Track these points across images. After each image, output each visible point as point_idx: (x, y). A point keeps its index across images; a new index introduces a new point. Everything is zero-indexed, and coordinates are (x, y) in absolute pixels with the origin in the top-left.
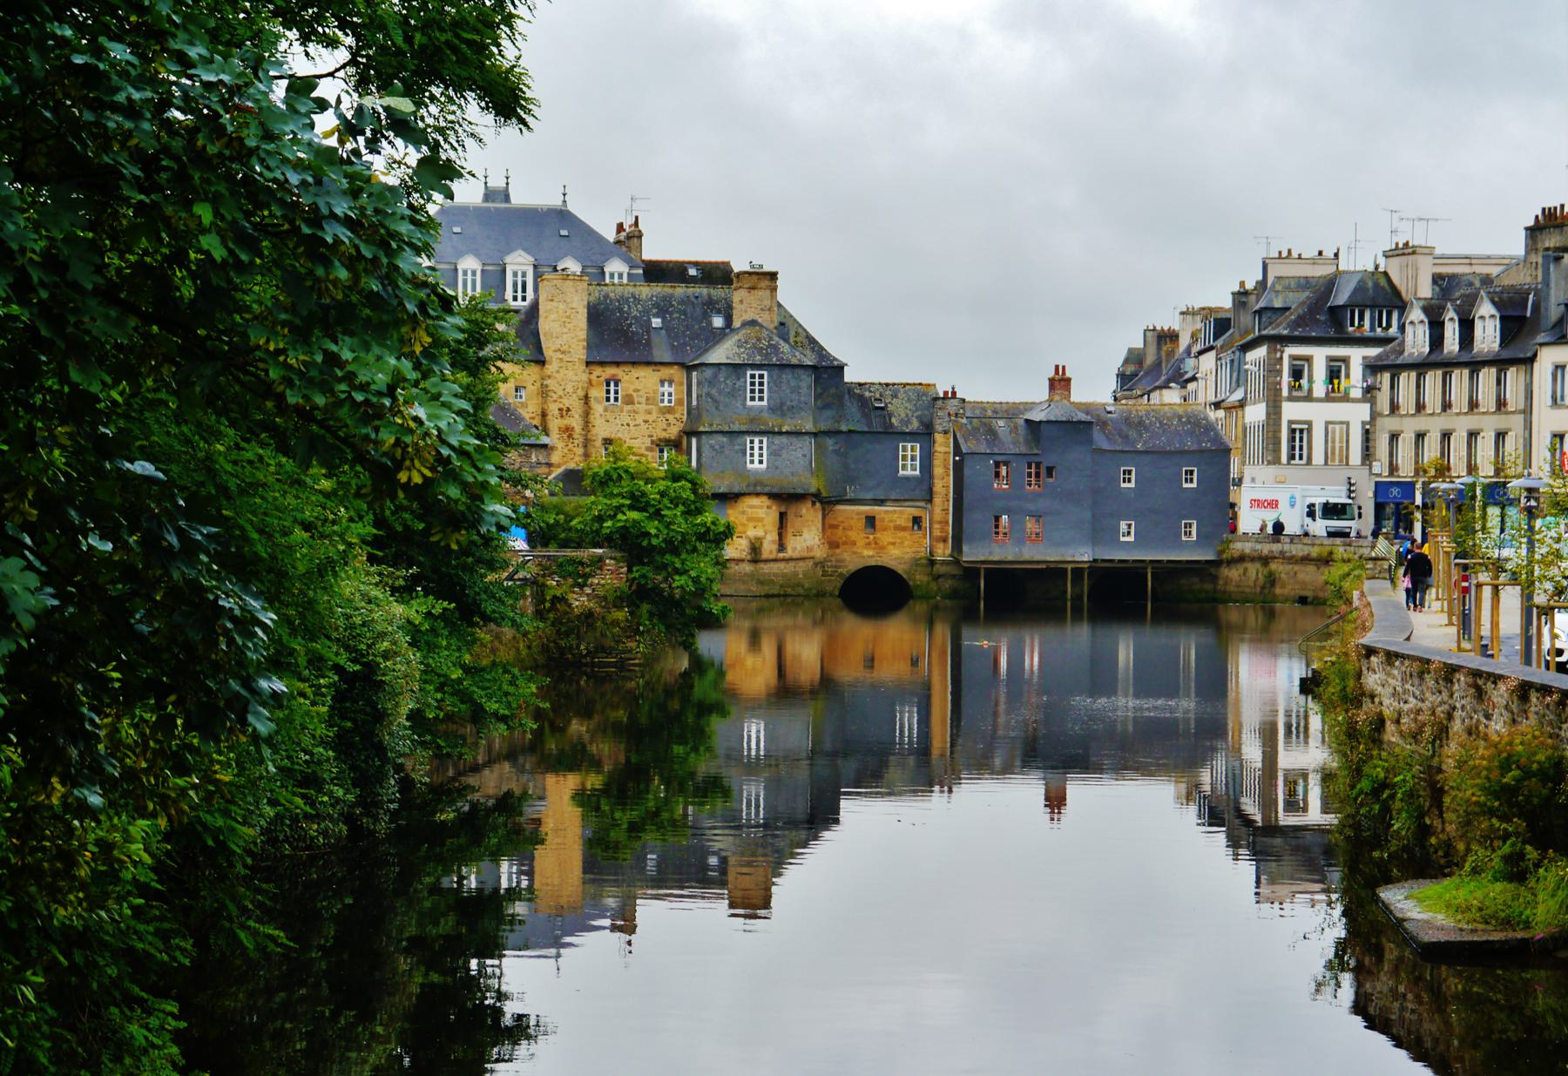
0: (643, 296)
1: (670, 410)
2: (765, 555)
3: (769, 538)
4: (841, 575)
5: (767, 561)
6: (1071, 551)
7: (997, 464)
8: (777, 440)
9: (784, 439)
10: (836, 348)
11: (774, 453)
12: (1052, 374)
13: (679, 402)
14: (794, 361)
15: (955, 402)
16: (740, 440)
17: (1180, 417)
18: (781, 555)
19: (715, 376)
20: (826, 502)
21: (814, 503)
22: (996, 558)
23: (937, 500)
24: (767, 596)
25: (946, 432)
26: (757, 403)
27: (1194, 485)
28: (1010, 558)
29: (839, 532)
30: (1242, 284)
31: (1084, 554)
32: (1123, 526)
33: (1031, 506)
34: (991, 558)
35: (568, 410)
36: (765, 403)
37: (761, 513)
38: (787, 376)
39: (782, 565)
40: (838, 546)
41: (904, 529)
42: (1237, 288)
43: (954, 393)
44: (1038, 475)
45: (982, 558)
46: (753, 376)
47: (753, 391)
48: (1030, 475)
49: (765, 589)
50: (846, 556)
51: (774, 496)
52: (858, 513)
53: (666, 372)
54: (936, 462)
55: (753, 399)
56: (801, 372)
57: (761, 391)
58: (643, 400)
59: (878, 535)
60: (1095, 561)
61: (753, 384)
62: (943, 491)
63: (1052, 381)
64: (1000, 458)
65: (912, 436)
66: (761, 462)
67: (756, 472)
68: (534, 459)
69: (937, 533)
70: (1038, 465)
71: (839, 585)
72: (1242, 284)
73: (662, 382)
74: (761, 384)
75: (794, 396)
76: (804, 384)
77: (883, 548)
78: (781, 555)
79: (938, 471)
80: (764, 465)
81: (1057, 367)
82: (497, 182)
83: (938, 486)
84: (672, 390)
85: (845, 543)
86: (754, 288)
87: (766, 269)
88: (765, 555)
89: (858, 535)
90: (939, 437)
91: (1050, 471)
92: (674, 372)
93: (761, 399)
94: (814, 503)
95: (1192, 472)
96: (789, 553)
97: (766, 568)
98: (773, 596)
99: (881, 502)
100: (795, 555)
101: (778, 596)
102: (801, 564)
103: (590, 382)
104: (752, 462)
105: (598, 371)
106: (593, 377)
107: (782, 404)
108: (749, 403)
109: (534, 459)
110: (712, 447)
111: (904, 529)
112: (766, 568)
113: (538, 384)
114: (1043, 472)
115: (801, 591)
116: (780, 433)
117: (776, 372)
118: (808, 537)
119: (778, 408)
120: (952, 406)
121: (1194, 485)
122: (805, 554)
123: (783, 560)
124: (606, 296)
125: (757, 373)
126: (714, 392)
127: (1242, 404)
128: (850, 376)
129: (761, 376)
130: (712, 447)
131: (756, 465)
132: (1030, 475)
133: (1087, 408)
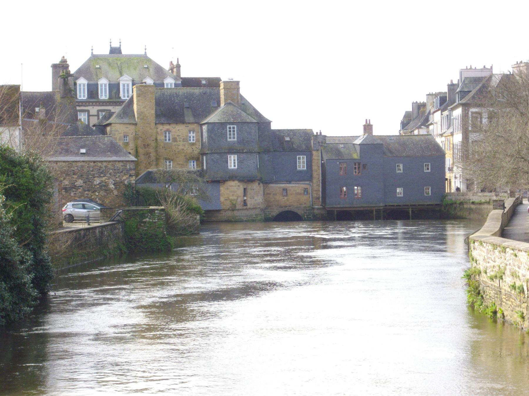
0: (181, 93)
1: (193, 144)
5: (238, 210)
8: (242, 156)
9: (244, 155)
10: (266, 114)
11: (240, 162)
12: (364, 123)
13: (197, 140)
14: (248, 121)
17: (423, 140)
20: (265, 182)
21: (259, 184)
23: (315, 181)
25: (317, 150)
26: (232, 140)
27: (429, 171)
29: (271, 196)
30: (452, 81)
32: (398, 190)
35: (148, 145)
36: (236, 139)
37: (235, 189)
42: (450, 83)
43: (321, 133)
46: (230, 128)
47: (230, 134)
48: (355, 168)
52: (279, 188)
53: (191, 127)
54: (313, 164)
55: (230, 138)
57: (234, 134)
58: (182, 140)
60: (386, 206)
61: (230, 131)
62: (317, 177)
63: (365, 126)
65: (302, 152)
66: (235, 166)
67: (233, 170)
68: (128, 167)
69: (315, 195)
70: (359, 164)
72: (452, 81)
73: (190, 132)
74: (234, 131)
78: (245, 207)
79: (315, 168)
80: (236, 167)
81: (366, 120)
82: (115, 45)
83: (315, 175)
84: (194, 135)
87: (235, 80)
88: (238, 207)
90: (314, 153)
91: (364, 166)
92: (195, 126)
93: (234, 138)
95: (428, 165)
96: (249, 206)
99: (289, 182)
100: (252, 207)
103: (157, 133)
106: (159, 130)
107: (243, 140)
108: (229, 140)
109: (128, 167)
111: (300, 194)
113: (134, 134)
114: (361, 166)
116: (243, 153)
119: (241, 141)
121: (429, 171)
123: (246, 209)
124: (164, 94)
125: (232, 126)
126: (213, 135)
127: (452, 134)
128: (274, 127)
129: (234, 128)
132: (355, 168)
133: (381, 138)
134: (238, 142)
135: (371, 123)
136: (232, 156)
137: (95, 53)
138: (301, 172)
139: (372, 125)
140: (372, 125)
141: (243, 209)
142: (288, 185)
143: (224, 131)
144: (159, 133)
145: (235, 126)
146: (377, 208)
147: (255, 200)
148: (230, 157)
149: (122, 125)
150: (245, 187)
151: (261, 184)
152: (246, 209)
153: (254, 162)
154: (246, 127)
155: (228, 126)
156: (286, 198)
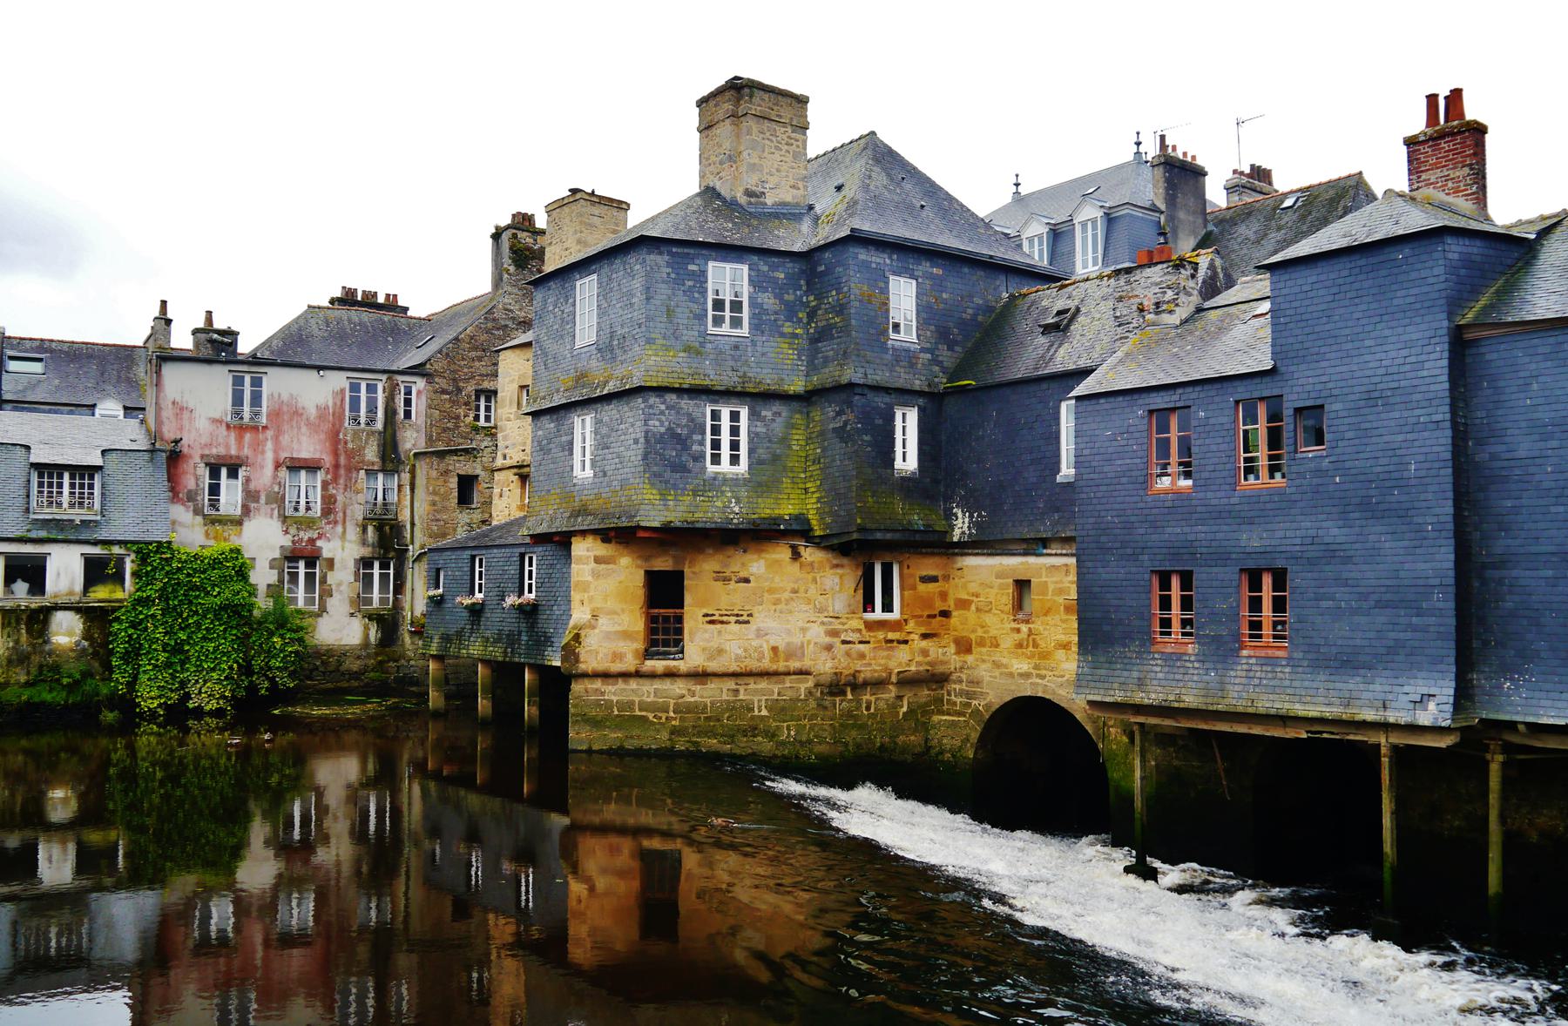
2: (588, 663)
3: (604, 623)
4: (976, 712)
5: (606, 676)
7: (1161, 416)
21: (796, 555)
22: (1152, 697)
24: (618, 753)
28: (1191, 700)
29: (971, 615)
31: (1422, 703)
33: (1253, 540)
34: (1140, 698)
39: (678, 687)
40: (969, 651)
45: (1118, 696)
49: (613, 737)
50: (984, 672)
51: (622, 535)
59: (1037, 625)
64: (1160, 401)
71: (975, 736)
76: (637, 284)
77: (1045, 656)
81: (1432, 99)
85: (981, 643)
86: (709, 127)
88: (588, 663)
89: (999, 624)
94: (796, 555)
97: (614, 692)
98: (640, 754)
100: (713, 666)
101: (666, 755)
102: (763, 684)
112: (614, 692)
115: (765, 746)
118: (781, 623)
122: (766, 664)
123: (671, 675)
135: (1471, 113)
136: (588, 419)
137: (1023, 190)
139: (1479, 130)
140: (1479, 130)
141: (638, 674)
142: (1031, 560)
147: (760, 634)
149: (518, 351)
150: (663, 564)
151: (810, 554)
152: (671, 675)
156: (1024, 628)
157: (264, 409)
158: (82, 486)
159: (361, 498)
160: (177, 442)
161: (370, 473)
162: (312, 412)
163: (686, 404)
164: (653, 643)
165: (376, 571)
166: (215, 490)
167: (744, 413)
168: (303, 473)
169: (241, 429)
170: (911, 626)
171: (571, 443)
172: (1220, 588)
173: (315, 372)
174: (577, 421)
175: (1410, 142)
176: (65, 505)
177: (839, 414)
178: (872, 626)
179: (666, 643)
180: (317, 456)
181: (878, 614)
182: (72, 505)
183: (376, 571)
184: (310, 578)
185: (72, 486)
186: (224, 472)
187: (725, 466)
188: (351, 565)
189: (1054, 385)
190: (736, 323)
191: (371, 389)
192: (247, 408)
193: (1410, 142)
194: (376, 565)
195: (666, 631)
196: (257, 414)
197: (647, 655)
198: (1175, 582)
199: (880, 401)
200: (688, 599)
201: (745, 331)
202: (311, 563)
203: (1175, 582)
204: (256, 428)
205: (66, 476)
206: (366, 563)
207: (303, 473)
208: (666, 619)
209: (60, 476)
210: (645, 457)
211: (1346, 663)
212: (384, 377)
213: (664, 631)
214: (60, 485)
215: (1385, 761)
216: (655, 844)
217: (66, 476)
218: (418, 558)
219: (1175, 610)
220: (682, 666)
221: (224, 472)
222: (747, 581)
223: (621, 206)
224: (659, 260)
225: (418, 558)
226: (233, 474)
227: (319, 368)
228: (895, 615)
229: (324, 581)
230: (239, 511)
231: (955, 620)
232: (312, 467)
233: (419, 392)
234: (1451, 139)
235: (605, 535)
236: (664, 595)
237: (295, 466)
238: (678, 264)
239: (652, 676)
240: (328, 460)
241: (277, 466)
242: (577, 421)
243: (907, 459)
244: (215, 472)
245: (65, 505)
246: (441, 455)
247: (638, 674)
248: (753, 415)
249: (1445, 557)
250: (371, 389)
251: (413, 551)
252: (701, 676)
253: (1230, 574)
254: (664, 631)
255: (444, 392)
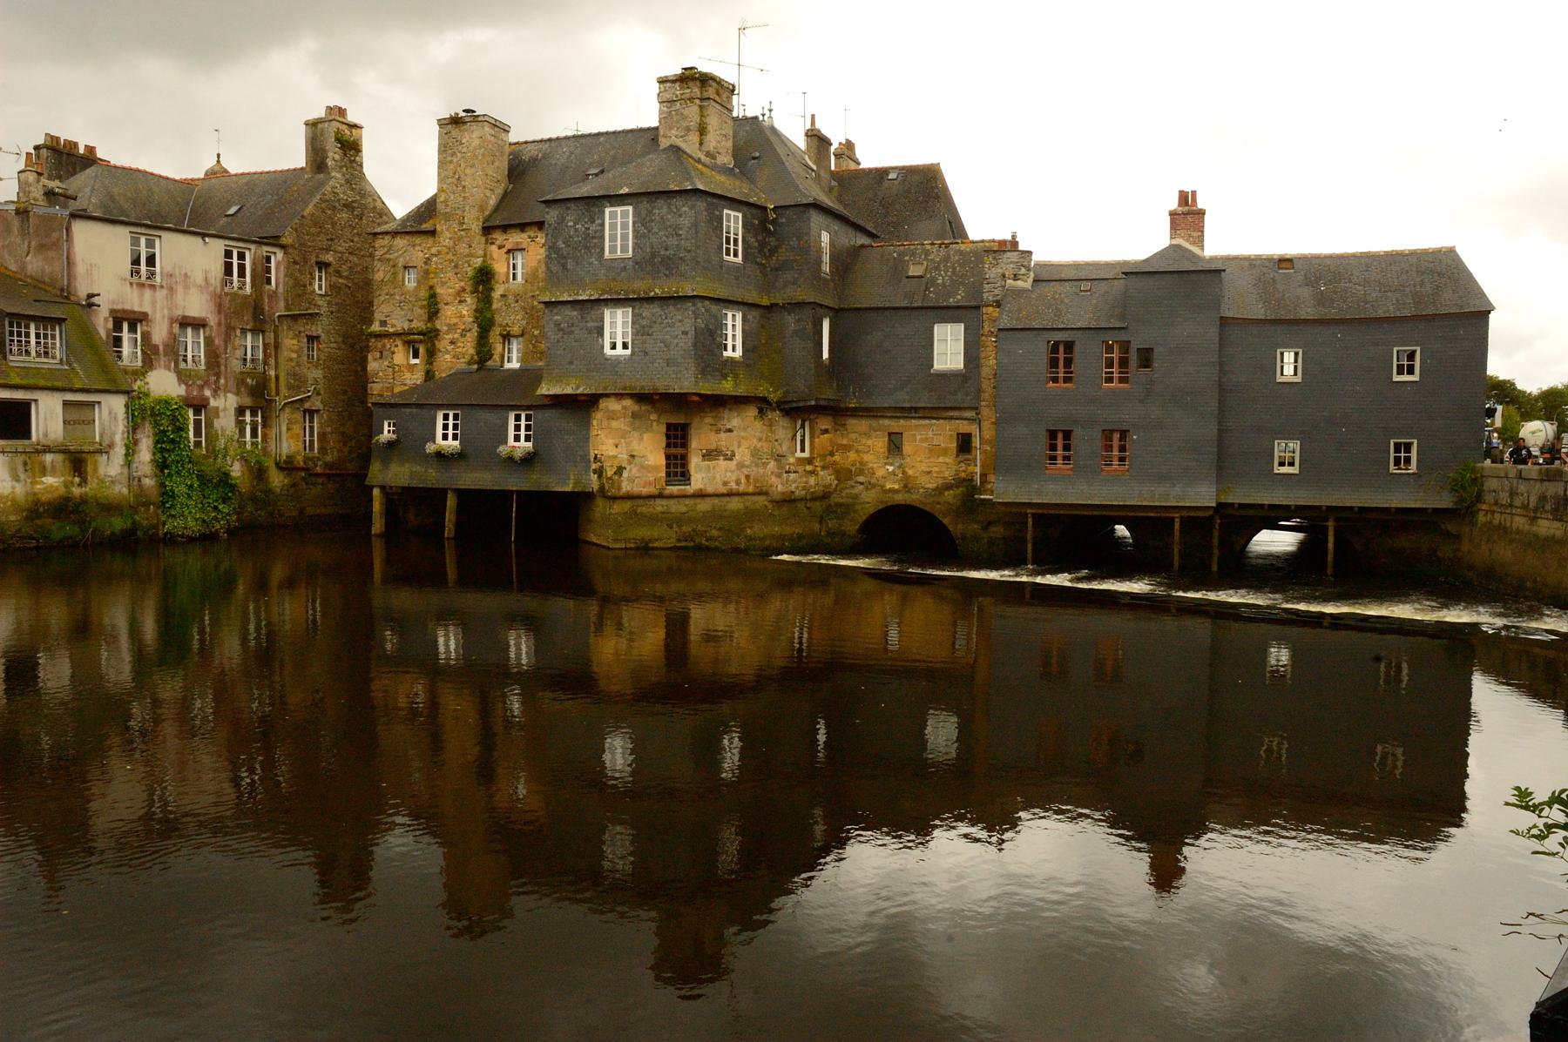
6: (1177, 490)
8: (649, 311)
9: (656, 309)
11: (641, 330)
12: (1173, 204)
15: (1013, 256)
16: (594, 313)
18: (674, 489)
19: (562, 220)
27: (1415, 378)
31: (1203, 495)
32: (1280, 448)
38: (661, 209)
41: (945, 452)
43: (1014, 243)
44: (1124, 363)
48: (1110, 364)
56: (678, 201)
75: (673, 241)
76: (685, 222)
78: (674, 489)
80: (628, 352)
91: (1146, 358)
104: (614, 347)
105: (499, 237)
107: (653, 255)
110: (557, 325)
117: (645, 204)
119: (650, 260)
120: (1008, 262)
125: (619, 209)
126: (560, 244)
130: (557, 325)
131: (619, 351)
132: (1110, 364)
134: (637, 262)
136: (619, 312)
138: (945, 376)
139: (1202, 213)
140: (1202, 213)
141: (661, 496)
143: (593, 228)
144: (495, 256)
145: (630, 208)
146: (1185, 514)
148: (613, 316)
153: (685, 333)
154: (665, 210)
155: (607, 211)
157: (158, 269)
158: (19, 334)
159: (239, 353)
160: (91, 296)
161: (244, 331)
162: (198, 277)
163: (714, 308)
164: (668, 474)
165: (248, 418)
166: (118, 342)
167: (739, 316)
168: (189, 330)
169: (141, 285)
170: (817, 463)
171: (602, 328)
172: (1087, 441)
173: (199, 240)
174: (607, 313)
175: (1172, 214)
176: (33, 353)
177: (799, 321)
178: (799, 459)
179: (676, 474)
180: (203, 315)
181: (799, 454)
182: (38, 355)
183: (248, 418)
184: (197, 423)
185: (38, 336)
186: (125, 326)
187: (728, 353)
188: (232, 412)
189: (932, 314)
190: (736, 255)
191: (241, 256)
192: (143, 267)
193: (1172, 214)
194: (248, 413)
195: (676, 466)
196: (153, 274)
197: (668, 483)
198: (1060, 436)
199: (820, 311)
200: (694, 444)
201: (739, 259)
202: (197, 412)
203: (1060, 436)
204: (153, 287)
205: (32, 326)
206: (240, 411)
207: (189, 330)
208: (676, 457)
209: (27, 327)
210: (695, 345)
211: (1161, 479)
212: (253, 247)
213: (677, 468)
214: (27, 335)
215: (1177, 525)
216: (676, 607)
217: (32, 326)
218: (282, 409)
219: (1060, 452)
220: (690, 489)
221: (125, 326)
222: (730, 431)
223: (505, 129)
224: (701, 205)
225: (282, 409)
226: (133, 329)
227: (203, 236)
228: (806, 454)
229: (209, 425)
230: (140, 364)
231: (837, 458)
232: (198, 324)
233: (278, 264)
234: (1187, 215)
235: (641, 398)
236: (677, 439)
237: (186, 323)
238: (711, 208)
239: (671, 497)
240: (212, 320)
241: (172, 321)
242: (607, 313)
243: (734, 349)
244: (118, 327)
245: (33, 353)
246: (294, 318)
247: (661, 496)
248: (744, 319)
249: (1213, 428)
250: (241, 256)
251: (280, 402)
252: (700, 495)
253: (1096, 434)
254: (677, 468)
255: (295, 262)
